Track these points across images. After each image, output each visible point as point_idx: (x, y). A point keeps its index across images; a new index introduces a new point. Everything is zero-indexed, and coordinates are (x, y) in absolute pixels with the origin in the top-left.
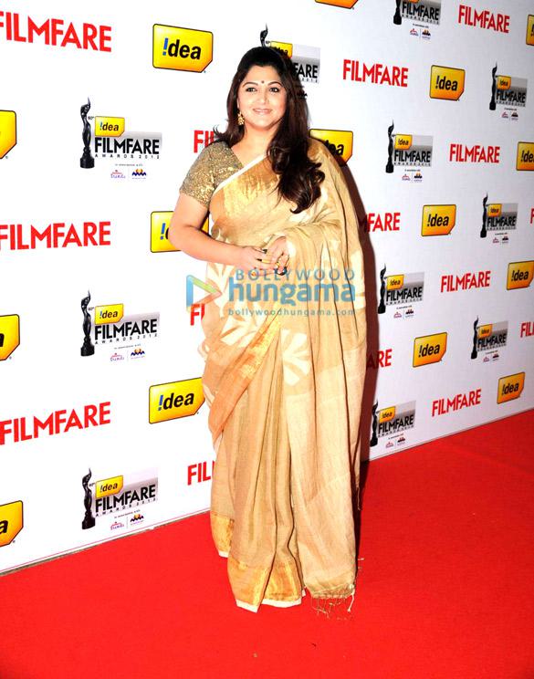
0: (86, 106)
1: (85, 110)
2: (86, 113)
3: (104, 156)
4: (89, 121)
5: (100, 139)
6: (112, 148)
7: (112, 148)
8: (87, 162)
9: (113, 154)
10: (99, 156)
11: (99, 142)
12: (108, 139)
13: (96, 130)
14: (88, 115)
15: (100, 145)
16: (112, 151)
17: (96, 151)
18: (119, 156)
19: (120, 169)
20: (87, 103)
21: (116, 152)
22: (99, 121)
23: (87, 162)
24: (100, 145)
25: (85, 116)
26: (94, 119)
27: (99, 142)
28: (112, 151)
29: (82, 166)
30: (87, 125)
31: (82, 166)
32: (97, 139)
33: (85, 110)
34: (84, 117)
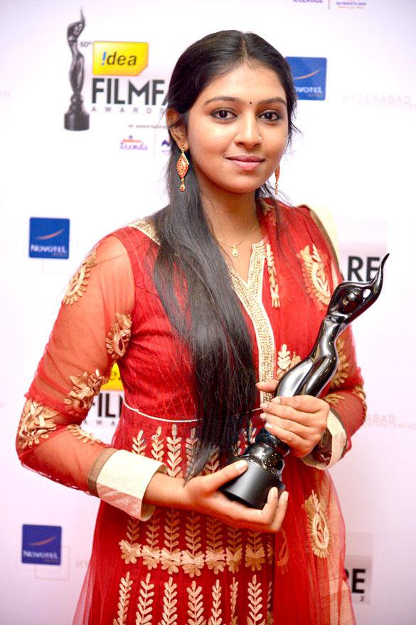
0: (78, 24)
1: (74, 32)
2: (77, 37)
3: (108, 110)
4: (82, 50)
5: (102, 80)
6: (123, 95)
7: (123, 95)
8: (77, 120)
9: (126, 106)
10: (96, 110)
11: (99, 85)
12: (117, 81)
13: (93, 66)
14: (81, 39)
15: (101, 90)
16: (123, 102)
17: (94, 101)
18: (136, 110)
19: (137, 134)
20: (78, 19)
21: (130, 102)
22: (100, 49)
23: (77, 120)
24: (101, 90)
25: (75, 41)
26: (90, 46)
27: (99, 85)
28: (123, 102)
29: (67, 126)
30: (79, 56)
31: (67, 126)
32: (95, 81)
33: (74, 32)
34: (72, 43)
